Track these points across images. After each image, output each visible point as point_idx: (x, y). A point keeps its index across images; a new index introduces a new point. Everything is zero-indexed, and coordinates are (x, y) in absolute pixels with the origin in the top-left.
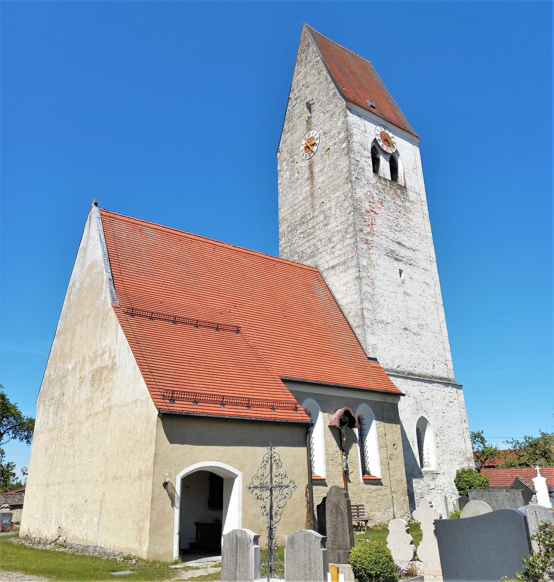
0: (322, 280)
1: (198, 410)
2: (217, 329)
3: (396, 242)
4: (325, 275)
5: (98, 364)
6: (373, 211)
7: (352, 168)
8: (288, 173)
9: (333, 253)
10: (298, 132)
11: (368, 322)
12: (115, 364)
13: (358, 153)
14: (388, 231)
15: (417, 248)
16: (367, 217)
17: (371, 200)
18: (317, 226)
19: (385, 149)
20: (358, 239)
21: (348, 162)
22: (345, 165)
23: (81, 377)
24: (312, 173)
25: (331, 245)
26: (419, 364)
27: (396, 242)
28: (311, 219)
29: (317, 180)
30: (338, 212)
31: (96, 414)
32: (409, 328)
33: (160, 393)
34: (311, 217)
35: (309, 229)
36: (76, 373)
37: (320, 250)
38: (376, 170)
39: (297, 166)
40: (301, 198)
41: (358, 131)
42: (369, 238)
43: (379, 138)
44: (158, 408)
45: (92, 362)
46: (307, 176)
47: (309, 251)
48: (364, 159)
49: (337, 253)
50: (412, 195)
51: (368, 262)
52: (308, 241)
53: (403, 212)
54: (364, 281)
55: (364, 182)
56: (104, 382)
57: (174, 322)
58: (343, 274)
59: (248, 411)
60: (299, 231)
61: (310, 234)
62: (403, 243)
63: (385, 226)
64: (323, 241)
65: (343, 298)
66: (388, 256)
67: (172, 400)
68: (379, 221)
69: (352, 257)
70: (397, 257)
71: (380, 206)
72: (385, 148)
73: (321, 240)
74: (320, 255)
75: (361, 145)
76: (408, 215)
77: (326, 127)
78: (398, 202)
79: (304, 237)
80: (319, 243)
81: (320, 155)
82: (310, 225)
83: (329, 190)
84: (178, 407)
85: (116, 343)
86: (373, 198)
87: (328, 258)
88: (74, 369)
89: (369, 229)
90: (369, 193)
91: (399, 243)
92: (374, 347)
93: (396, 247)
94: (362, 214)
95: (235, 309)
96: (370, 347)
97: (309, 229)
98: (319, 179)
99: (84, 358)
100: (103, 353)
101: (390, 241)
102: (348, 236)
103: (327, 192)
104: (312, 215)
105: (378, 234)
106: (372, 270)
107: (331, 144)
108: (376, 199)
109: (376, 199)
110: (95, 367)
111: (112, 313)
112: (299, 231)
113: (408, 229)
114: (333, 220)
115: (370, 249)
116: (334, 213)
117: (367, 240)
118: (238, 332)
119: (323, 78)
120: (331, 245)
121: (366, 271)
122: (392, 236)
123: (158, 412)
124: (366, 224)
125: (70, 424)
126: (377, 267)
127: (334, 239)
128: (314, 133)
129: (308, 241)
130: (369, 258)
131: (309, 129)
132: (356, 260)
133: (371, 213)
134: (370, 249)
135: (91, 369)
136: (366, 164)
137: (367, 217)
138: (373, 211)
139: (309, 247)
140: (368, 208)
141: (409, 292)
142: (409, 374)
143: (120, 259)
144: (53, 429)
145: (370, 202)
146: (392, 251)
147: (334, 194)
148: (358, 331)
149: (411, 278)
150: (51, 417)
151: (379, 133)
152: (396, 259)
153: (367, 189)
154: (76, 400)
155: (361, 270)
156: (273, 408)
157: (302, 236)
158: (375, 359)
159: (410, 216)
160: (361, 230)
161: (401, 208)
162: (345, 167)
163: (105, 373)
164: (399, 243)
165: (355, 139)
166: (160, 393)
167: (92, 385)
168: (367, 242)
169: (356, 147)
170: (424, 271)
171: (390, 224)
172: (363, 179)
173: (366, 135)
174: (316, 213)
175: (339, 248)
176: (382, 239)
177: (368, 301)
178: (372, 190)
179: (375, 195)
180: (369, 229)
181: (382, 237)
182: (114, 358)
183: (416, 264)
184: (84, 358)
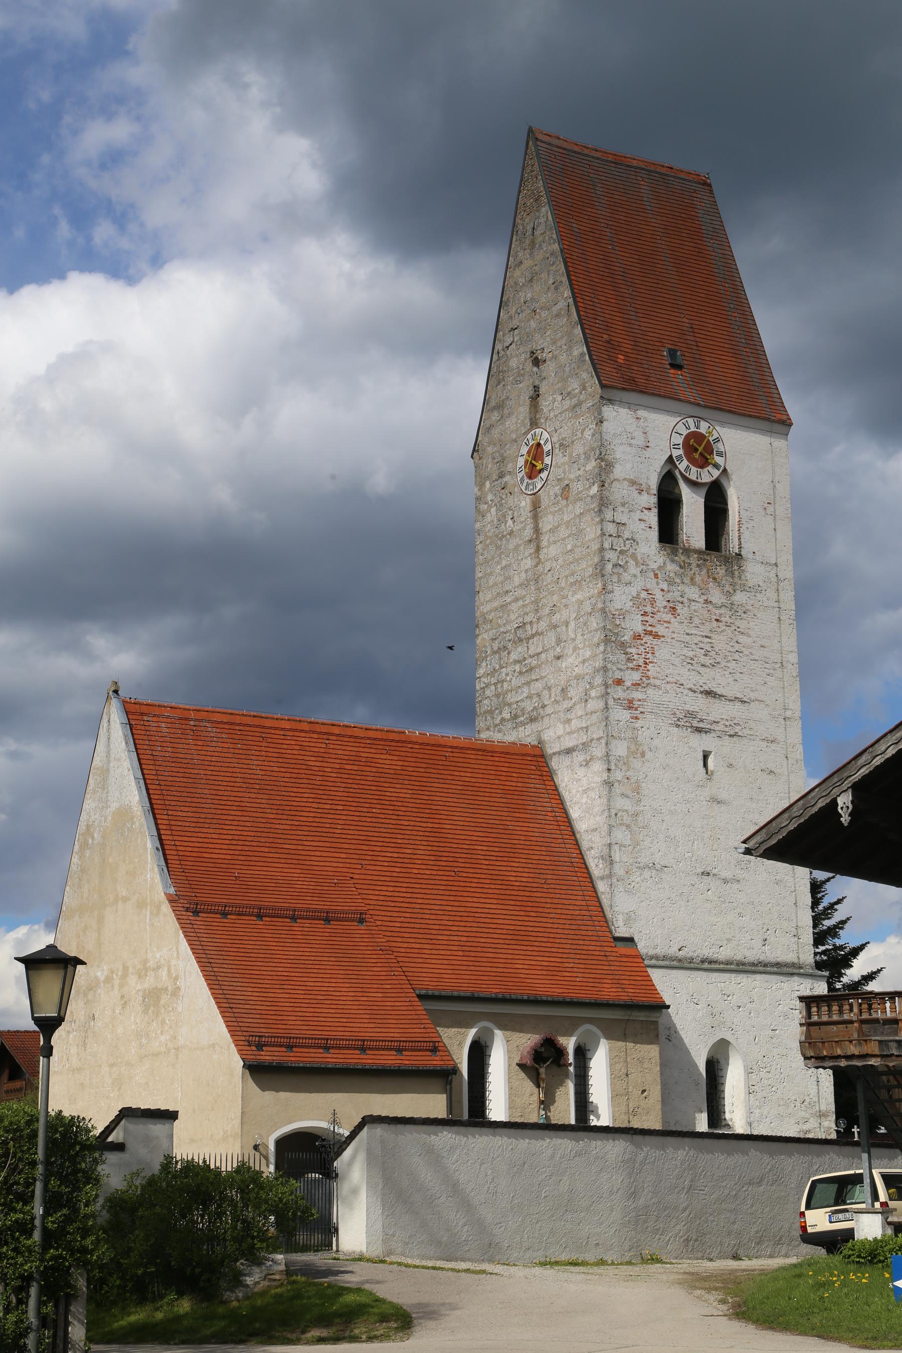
0: (547, 776)
1: (293, 1059)
2: (327, 920)
3: (701, 692)
4: (554, 763)
5: (149, 982)
6: (647, 633)
7: (607, 545)
8: (493, 510)
9: (568, 721)
10: (513, 419)
11: (619, 870)
12: (179, 988)
13: (623, 505)
14: (684, 671)
15: (753, 696)
16: (633, 650)
17: (649, 609)
18: (543, 656)
19: (693, 477)
20: (611, 702)
21: (599, 532)
22: (592, 536)
23: (122, 997)
24: (537, 530)
25: (566, 704)
26: (729, 940)
27: (701, 692)
28: (533, 636)
29: (545, 550)
30: (579, 637)
31: (157, 1054)
32: (714, 871)
33: (243, 1038)
34: (534, 632)
35: (531, 657)
36: (113, 986)
37: (549, 710)
38: (668, 532)
39: (511, 501)
40: (517, 581)
41: (628, 449)
42: (637, 695)
43: (681, 452)
44: (243, 1059)
45: (140, 977)
46: (528, 532)
47: (528, 706)
48: (638, 515)
49: (575, 724)
50: (753, 572)
51: (628, 748)
52: (528, 683)
53: (727, 619)
54: (618, 789)
55: (633, 569)
56: (163, 1011)
57: (260, 916)
58: (583, 769)
59: (361, 1056)
60: (514, 656)
61: (531, 670)
62: (719, 691)
63: (677, 661)
64: (553, 690)
65: (581, 818)
66: (678, 726)
67: (260, 1046)
68: (663, 652)
69: (599, 739)
70: (701, 725)
71: (668, 617)
72: (693, 473)
73: (549, 688)
74: (546, 720)
75: (633, 483)
76: (738, 623)
77: (565, 432)
78: (716, 596)
79: (521, 673)
80: (546, 692)
81: (552, 493)
82: (532, 651)
83: (566, 581)
84: (267, 1056)
85: (178, 958)
86: (653, 602)
87: (560, 729)
88: (108, 980)
89: (636, 676)
90: (644, 595)
91: (709, 693)
92: (629, 919)
93: (699, 704)
94: (623, 645)
95: (363, 871)
96: (620, 917)
97: (531, 657)
98: (550, 551)
99: (126, 968)
100: (158, 967)
101: (686, 692)
102: (593, 693)
103: (563, 585)
104: (535, 626)
105: (658, 682)
106: (636, 763)
107: (572, 476)
108: (661, 602)
109: (661, 602)
110: (146, 986)
111: (166, 908)
112: (514, 656)
113: (736, 656)
114: (571, 651)
115: (637, 718)
116: (573, 636)
117: (631, 701)
118: (361, 921)
119: (562, 304)
120: (566, 704)
121: (624, 768)
122: (691, 679)
123: (242, 1063)
124: (630, 665)
125: (112, 1065)
126: (649, 755)
127: (572, 692)
128: (543, 435)
129: (528, 683)
130: (634, 739)
131: (534, 424)
132: (604, 745)
133: (648, 639)
134: (637, 718)
135: (139, 987)
136: (642, 525)
137: (633, 650)
138: (647, 633)
139: (530, 697)
140: (639, 629)
141: (723, 796)
142: (703, 962)
143: (167, 803)
144: (79, 1070)
145: (645, 614)
146: (690, 714)
147: (575, 593)
148: (601, 887)
149: (730, 766)
150: (74, 1050)
151: (685, 432)
152: (699, 730)
153: (639, 584)
154: (120, 1031)
155: (613, 767)
156: (399, 1050)
157: (517, 667)
158: (631, 940)
159: (743, 625)
160: (619, 682)
161: (723, 611)
162: (594, 540)
163: (165, 999)
164: (709, 693)
165: (618, 471)
166: (243, 1038)
167: (145, 1012)
168: (630, 705)
169: (619, 491)
170: (765, 744)
171: (691, 654)
172: (632, 563)
173: (648, 453)
174: (543, 625)
175: (579, 714)
176: (667, 692)
177: (624, 828)
178: (651, 583)
179: (658, 595)
180: (636, 676)
181: (668, 687)
182: (176, 978)
183: (746, 732)
184: (126, 968)
